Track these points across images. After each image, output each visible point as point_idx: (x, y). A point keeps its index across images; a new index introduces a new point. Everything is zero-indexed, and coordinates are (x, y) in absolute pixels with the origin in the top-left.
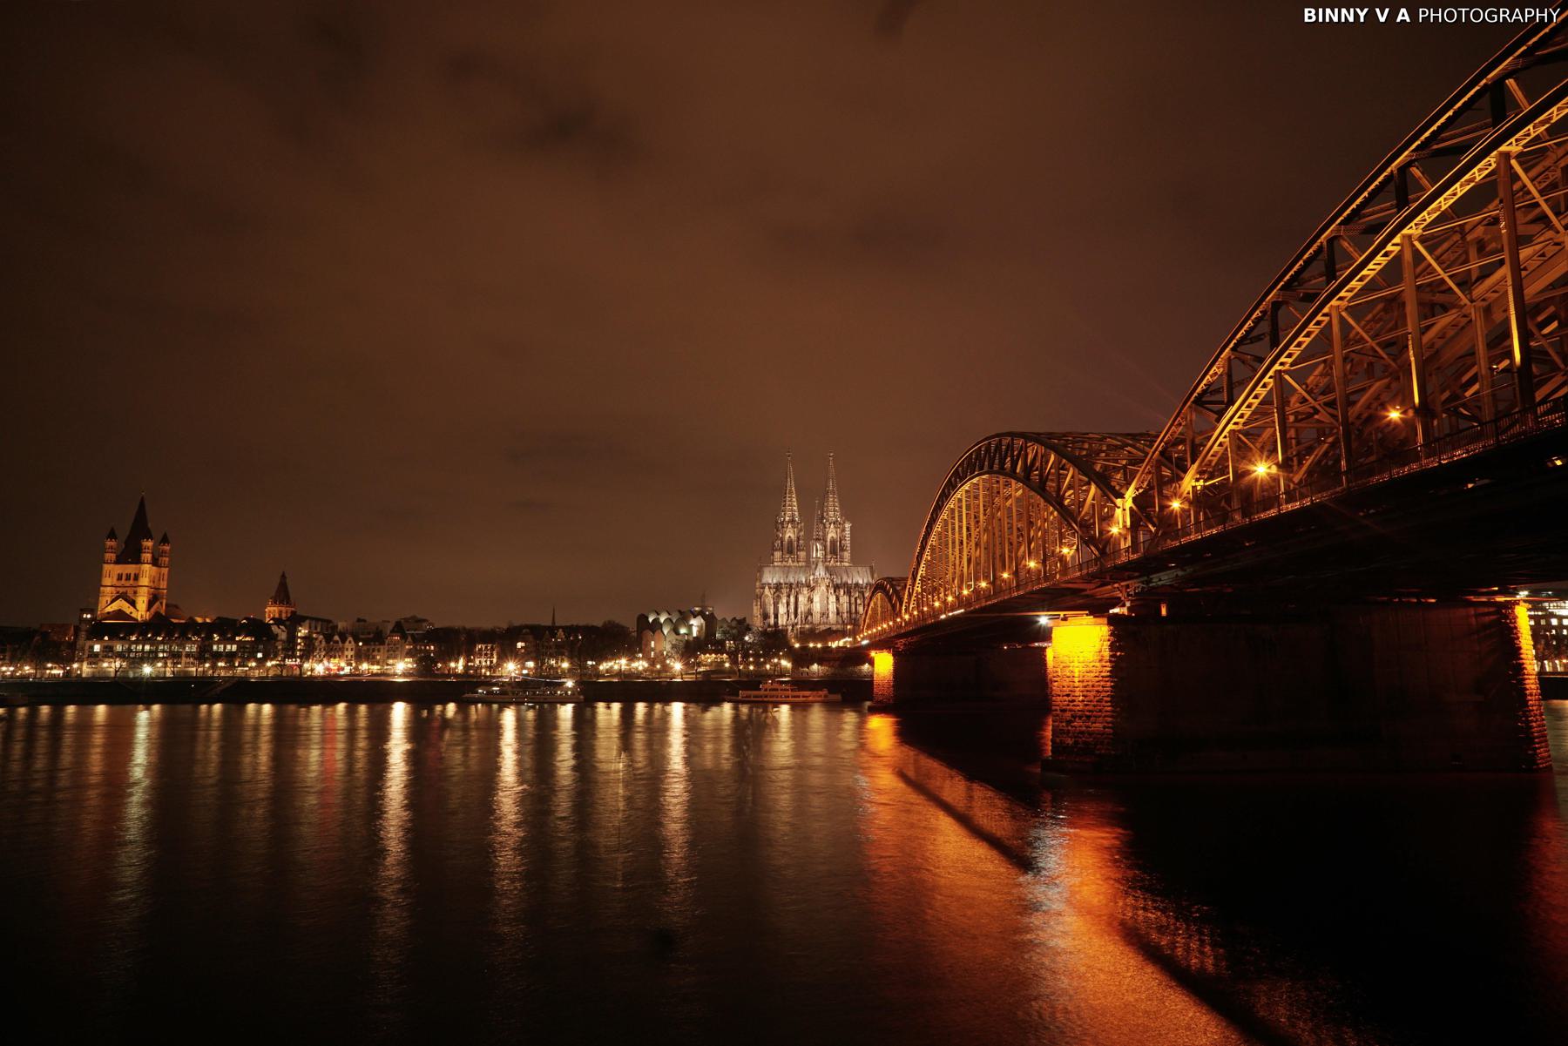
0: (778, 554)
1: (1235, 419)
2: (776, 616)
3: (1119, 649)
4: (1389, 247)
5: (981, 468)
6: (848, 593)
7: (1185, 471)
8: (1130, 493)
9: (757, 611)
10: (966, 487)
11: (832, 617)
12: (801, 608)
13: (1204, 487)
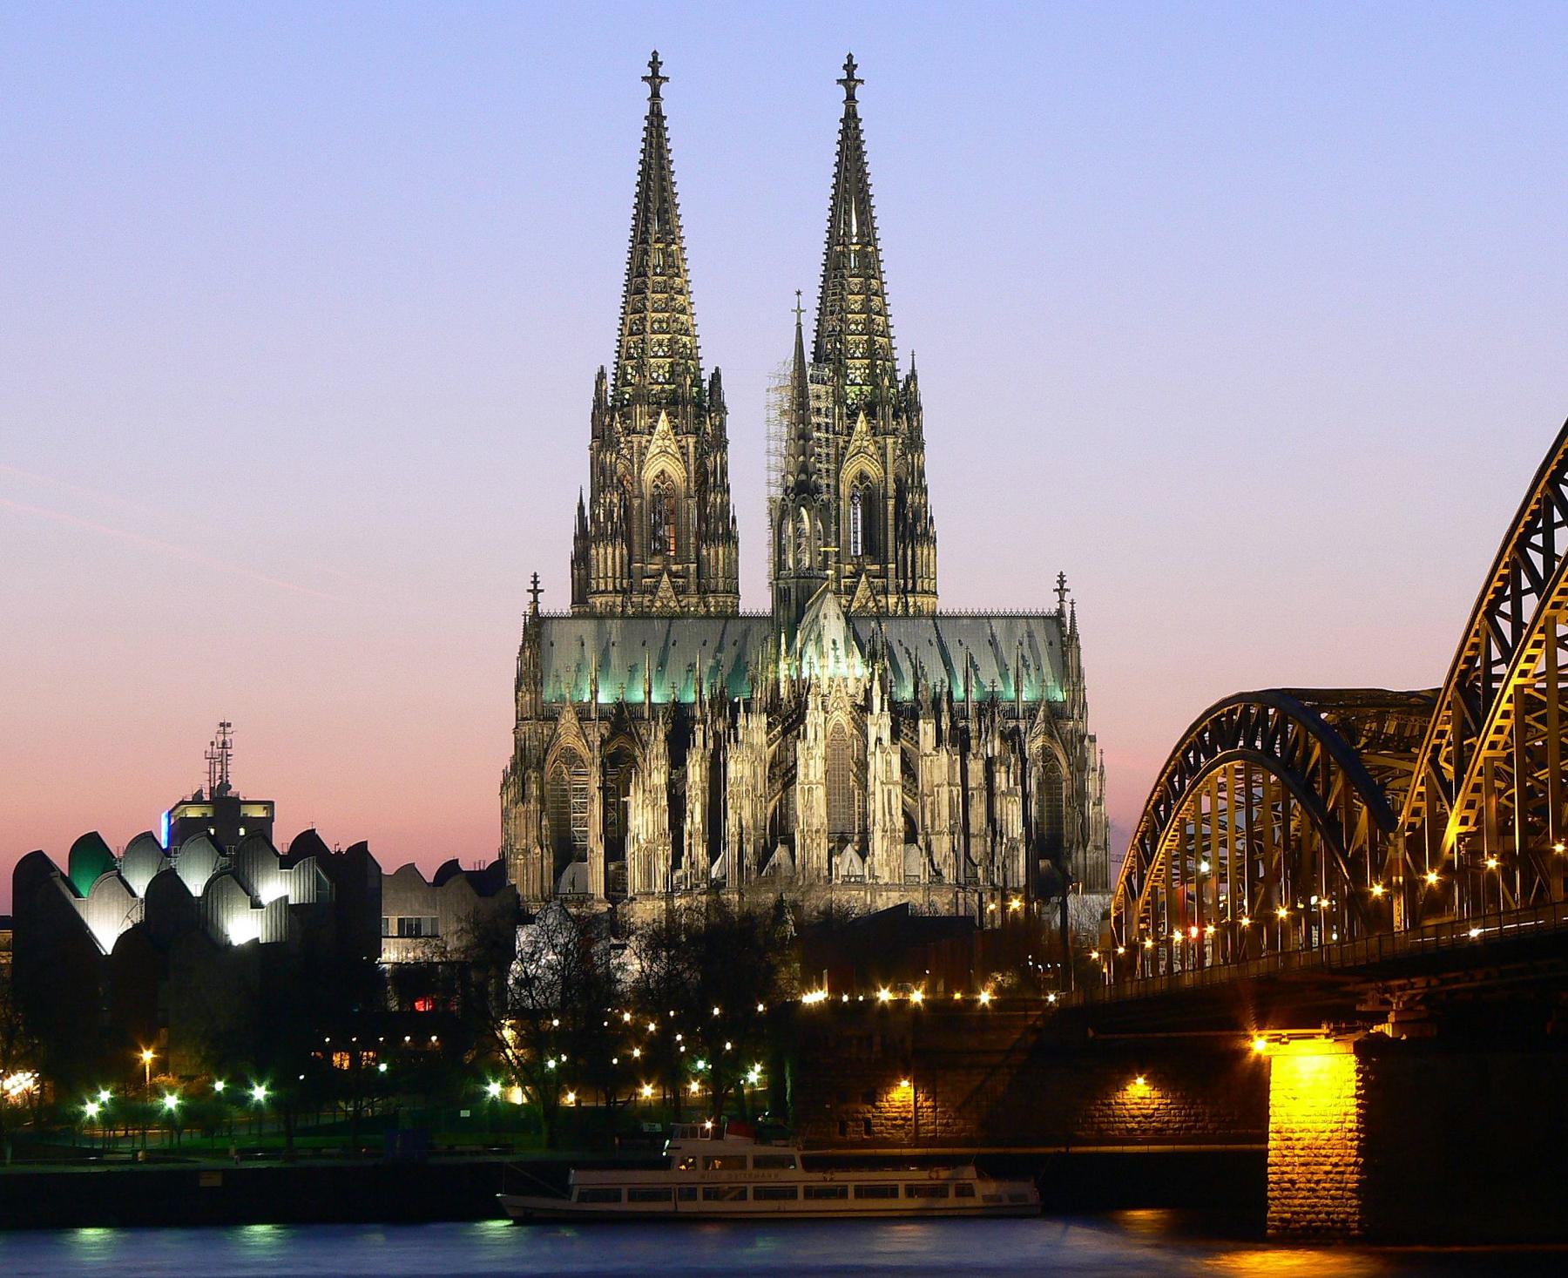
2: (615, 848)
6: (960, 741)
12: (742, 813)
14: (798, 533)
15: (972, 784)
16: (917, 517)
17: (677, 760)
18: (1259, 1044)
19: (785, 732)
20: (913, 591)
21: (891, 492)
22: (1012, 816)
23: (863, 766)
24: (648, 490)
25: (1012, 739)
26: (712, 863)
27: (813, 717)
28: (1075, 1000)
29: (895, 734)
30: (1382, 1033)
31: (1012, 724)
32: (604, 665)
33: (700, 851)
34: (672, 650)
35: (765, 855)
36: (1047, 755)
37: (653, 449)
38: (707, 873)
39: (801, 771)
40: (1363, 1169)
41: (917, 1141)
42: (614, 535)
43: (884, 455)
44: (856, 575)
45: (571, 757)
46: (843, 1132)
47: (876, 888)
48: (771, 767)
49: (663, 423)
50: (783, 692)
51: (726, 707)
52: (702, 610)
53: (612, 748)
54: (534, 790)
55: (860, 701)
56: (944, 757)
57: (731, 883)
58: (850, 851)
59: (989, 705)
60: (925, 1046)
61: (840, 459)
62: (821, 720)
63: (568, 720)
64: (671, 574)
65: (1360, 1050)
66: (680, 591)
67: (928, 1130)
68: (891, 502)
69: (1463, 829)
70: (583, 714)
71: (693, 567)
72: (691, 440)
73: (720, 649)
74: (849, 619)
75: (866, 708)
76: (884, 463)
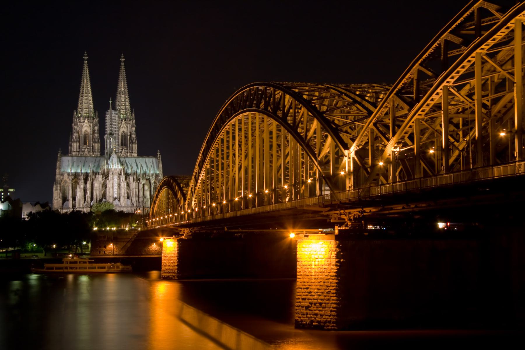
0: (75, 146)
1: (419, 112)
2: (74, 199)
3: (343, 257)
4: (509, 25)
6: (138, 180)
7: (388, 140)
8: (353, 148)
10: (239, 117)
12: (97, 194)
13: (400, 153)
14: (110, 141)
17: (85, 183)
18: (161, 239)
19: (106, 178)
22: (147, 194)
24: (83, 133)
25: (149, 180)
27: (110, 176)
28: (143, 230)
29: (126, 179)
30: (182, 239)
32: (73, 165)
33: (89, 200)
34: (86, 163)
35: (101, 201)
36: (155, 183)
37: (84, 126)
39: (108, 186)
40: (178, 262)
41: (113, 255)
44: (122, 149)
45: (66, 182)
46: (100, 253)
47: (121, 207)
49: (86, 121)
50: (105, 171)
51: (95, 174)
53: (74, 181)
54: (59, 188)
56: (135, 183)
58: (117, 200)
59: (145, 174)
60: (115, 237)
61: (119, 128)
63: (66, 175)
65: (178, 241)
66: (89, 152)
67: (115, 253)
70: (69, 174)
72: (92, 124)
73: (95, 163)
74: (119, 158)
75: (120, 174)
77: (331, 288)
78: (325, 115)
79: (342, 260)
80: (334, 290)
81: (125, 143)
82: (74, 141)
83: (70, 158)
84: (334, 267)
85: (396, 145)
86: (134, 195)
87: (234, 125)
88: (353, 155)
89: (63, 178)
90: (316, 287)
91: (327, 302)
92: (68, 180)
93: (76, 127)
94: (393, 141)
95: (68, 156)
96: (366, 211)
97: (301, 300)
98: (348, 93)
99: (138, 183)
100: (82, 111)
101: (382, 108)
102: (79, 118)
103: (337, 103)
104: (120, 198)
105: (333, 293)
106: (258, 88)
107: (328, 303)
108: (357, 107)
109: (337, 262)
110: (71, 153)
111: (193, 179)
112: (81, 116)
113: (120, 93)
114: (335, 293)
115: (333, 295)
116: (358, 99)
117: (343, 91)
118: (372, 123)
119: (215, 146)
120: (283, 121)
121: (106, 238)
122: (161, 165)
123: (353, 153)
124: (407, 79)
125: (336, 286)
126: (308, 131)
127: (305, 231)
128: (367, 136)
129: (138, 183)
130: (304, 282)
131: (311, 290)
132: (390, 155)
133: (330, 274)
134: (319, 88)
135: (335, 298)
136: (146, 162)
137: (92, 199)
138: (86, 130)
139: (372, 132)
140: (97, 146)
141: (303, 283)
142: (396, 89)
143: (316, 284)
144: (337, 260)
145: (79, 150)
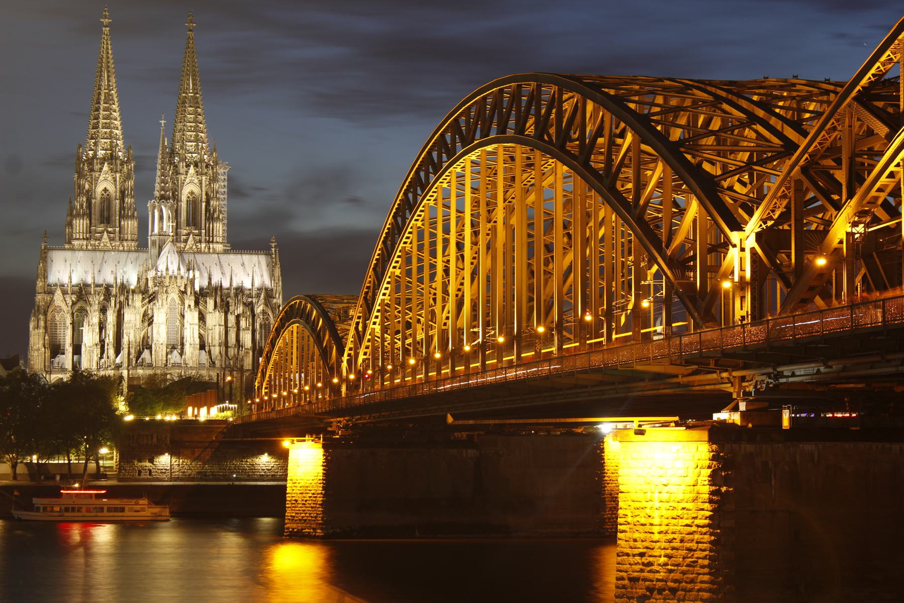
0: (80, 224)
2: (77, 350)
3: (726, 481)
5: (502, 130)
6: (225, 307)
7: (838, 207)
8: (753, 225)
9: (37, 340)
10: (473, 156)
11: (191, 350)
12: (131, 335)
13: (866, 236)
15: (229, 325)
16: (214, 211)
18: (286, 443)
20: (212, 242)
21: (204, 200)
23: (183, 316)
24: (98, 196)
25: (250, 306)
26: (117, 357)
27: (161, 297)
29: (197, 303)
31: (250, 300)
33: (111, 352)
36: (264, 312)
37: (101, 178)
38: (114, 361)
39: (155, 319)
40: (324, 495)
41: (171, 479)
42: (83, 215)
43: (201, 184)
44: (188, 234)
46: (139, 475)
48: (144, 316)
49: (106, 168)
52: (121, 248)
55: (182, 289)
57: (125, 365)
58: (175, 352)
62: (165, 297)
63: (58, 293)
64: (108, 232)
65: (324, 446)
66: (111, 239)
68: (204, 204)
69: (365, 357)
71: (117, 229)
72: (118, 175)
74: (181, 253)
75: (184, 293)
76: (201, 187)
77: (698, 554)
78: (682, 149)
79: (724, 489)
80: (705, 558)
81: (194, 218)
82: (78, 215)
83: (68, 254)
84: (707, 506)
85: (856, 219)
86: (217, 342)
87: (461, 176)
88: (751, 242)
89: (52, 300)
90: (663, 552)
91: (689, 586)
92: (63, 305)
93: (82, 182)
94: (849, 209)
95: (65, 249)
96: (785, 374)
97: (626, 582)
98: (734, 99)
99: (226, 314)
100: (96, 144)
101: (823, 133)
102: (90, 162)
103: (708, 122)
104: (182, 349)
105: (703, 567)
106: (519, 86)
107: (691, 590)
108: (756, 131)
109: (712, 493)
110: (70, 243)
111: (361, 301)
112: (95, 155)
113: (184, 102)
114: (708, 566)
115: (702, 571)
116: (761, 113)
117: (724, 94)
118: (797, 168)
119: (415, 222)
120: (579, 162)
121: (155, 440)
122: (278, 272)
123: (753, 236)
124: (883, 64)
125: (711, 551)
126: (640, 185)
127: (636, 420)
128: (784, 196)
129: (226, 314)
130: (635, 540)
131: (651, 559)
132: (841, 242)
133: (697, 522)
134: (665, 88)
135: (706, 578)
136: (243, 264)
137: (118, 352)
138: (105, 190)
139: (800, 190)
140: (131, 226)
141: (632, 543)
142: (858, 88)
143: (663, 545)
144: (714, 488)
145: (90, 235)
